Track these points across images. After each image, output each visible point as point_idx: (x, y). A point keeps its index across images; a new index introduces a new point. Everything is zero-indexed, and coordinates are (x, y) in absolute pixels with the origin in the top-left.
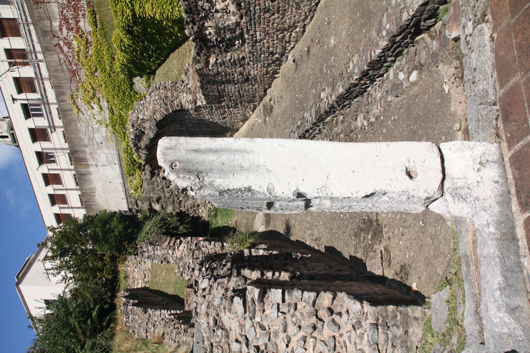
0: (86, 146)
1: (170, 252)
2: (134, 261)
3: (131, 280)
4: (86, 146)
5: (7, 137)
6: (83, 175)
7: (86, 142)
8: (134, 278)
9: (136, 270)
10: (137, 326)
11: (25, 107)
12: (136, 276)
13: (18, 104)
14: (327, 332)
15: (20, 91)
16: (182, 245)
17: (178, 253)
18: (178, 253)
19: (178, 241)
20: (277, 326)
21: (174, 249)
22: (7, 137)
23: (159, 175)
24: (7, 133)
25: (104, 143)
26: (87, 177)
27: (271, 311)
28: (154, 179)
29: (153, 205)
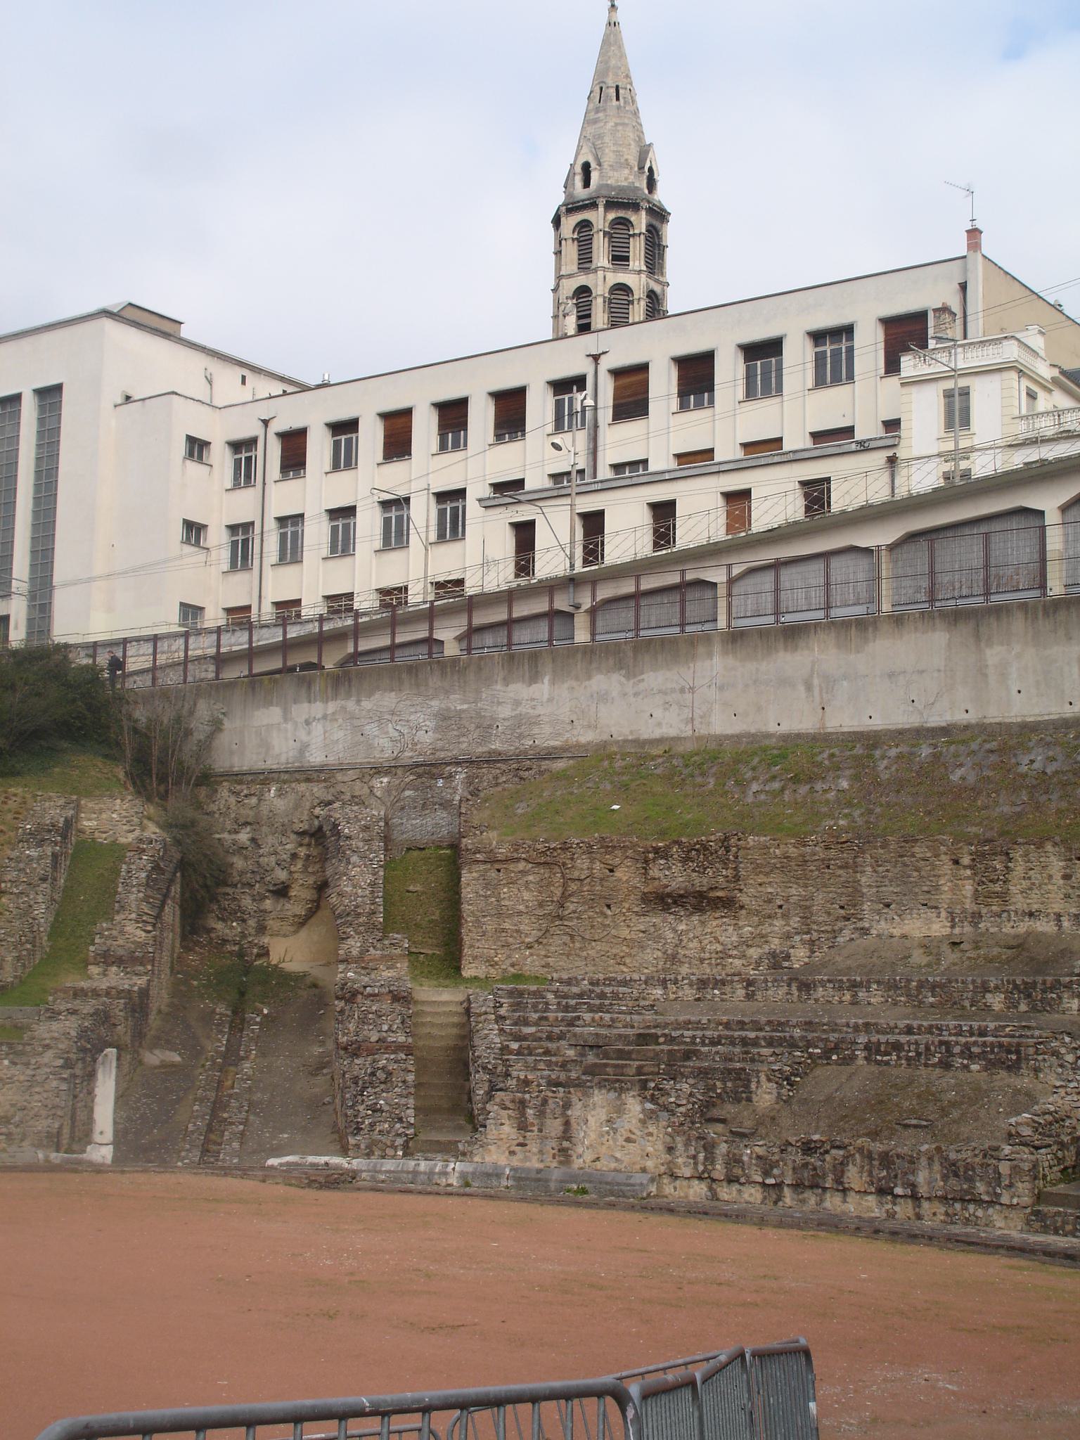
0: (359, 701)
1: (133, 916)
2: (132, 812)
3: (97, 807)
4: (359, 701)
5: (587, 183)
6: (309, 687)
7: (367, 704)
8: (101, 811)
9: (114, 816)
10: (22, 866)
11: (579, 382)
12: (104, 816)
13: (586, 367)
14: (44, 1113)
15: (617, 373)
16: (144, 934)
17: (130, 928)
18: (130, 928)
19: (150, 928)
20: (47, 1087)
21: (138, 922)
22: (587, 183)
23: (301, 845)
24: (600, 187)
25: (362, 739)
26: (304, 691)
27: (55, 1083)
28: (293, 837)
29: (248, 829)
